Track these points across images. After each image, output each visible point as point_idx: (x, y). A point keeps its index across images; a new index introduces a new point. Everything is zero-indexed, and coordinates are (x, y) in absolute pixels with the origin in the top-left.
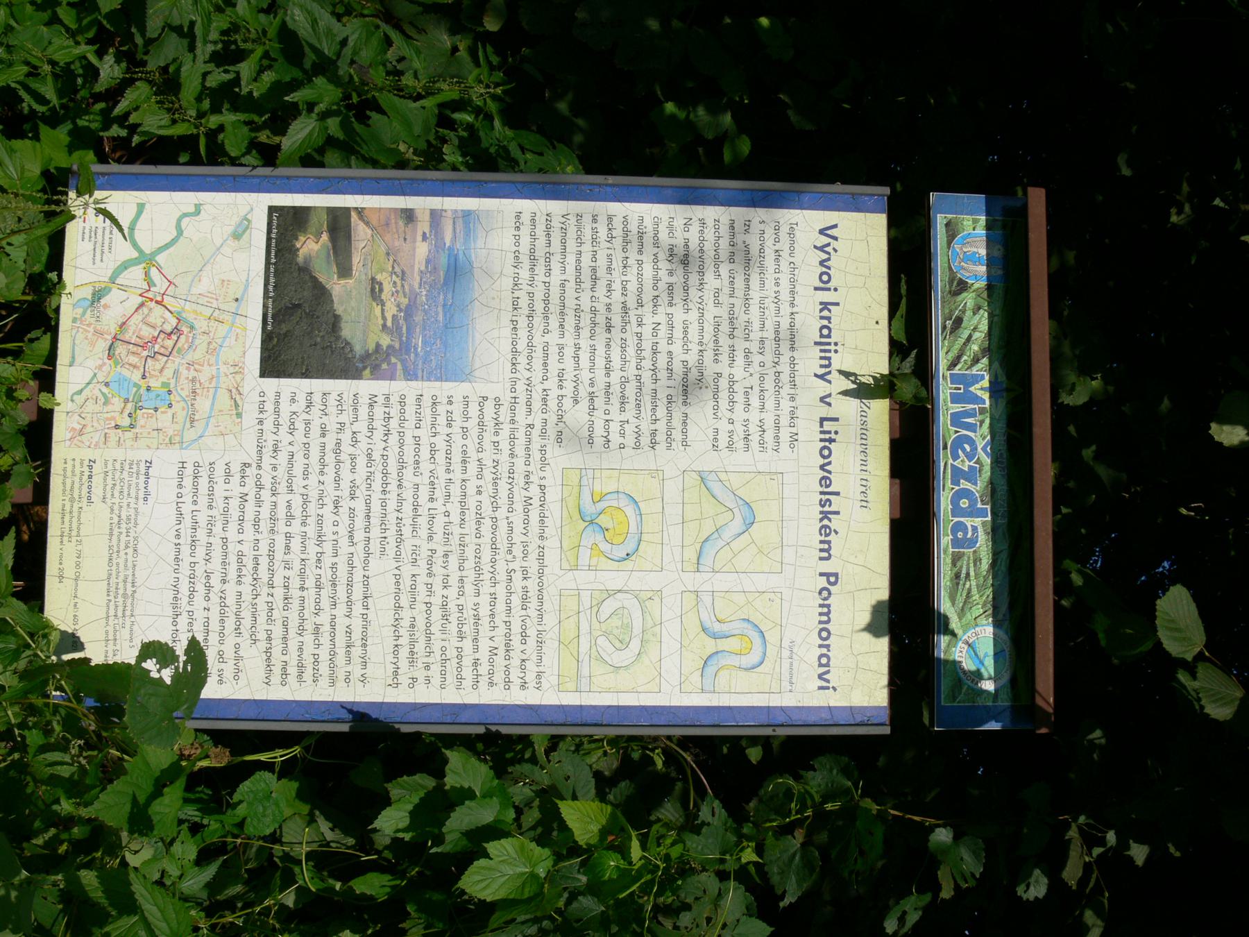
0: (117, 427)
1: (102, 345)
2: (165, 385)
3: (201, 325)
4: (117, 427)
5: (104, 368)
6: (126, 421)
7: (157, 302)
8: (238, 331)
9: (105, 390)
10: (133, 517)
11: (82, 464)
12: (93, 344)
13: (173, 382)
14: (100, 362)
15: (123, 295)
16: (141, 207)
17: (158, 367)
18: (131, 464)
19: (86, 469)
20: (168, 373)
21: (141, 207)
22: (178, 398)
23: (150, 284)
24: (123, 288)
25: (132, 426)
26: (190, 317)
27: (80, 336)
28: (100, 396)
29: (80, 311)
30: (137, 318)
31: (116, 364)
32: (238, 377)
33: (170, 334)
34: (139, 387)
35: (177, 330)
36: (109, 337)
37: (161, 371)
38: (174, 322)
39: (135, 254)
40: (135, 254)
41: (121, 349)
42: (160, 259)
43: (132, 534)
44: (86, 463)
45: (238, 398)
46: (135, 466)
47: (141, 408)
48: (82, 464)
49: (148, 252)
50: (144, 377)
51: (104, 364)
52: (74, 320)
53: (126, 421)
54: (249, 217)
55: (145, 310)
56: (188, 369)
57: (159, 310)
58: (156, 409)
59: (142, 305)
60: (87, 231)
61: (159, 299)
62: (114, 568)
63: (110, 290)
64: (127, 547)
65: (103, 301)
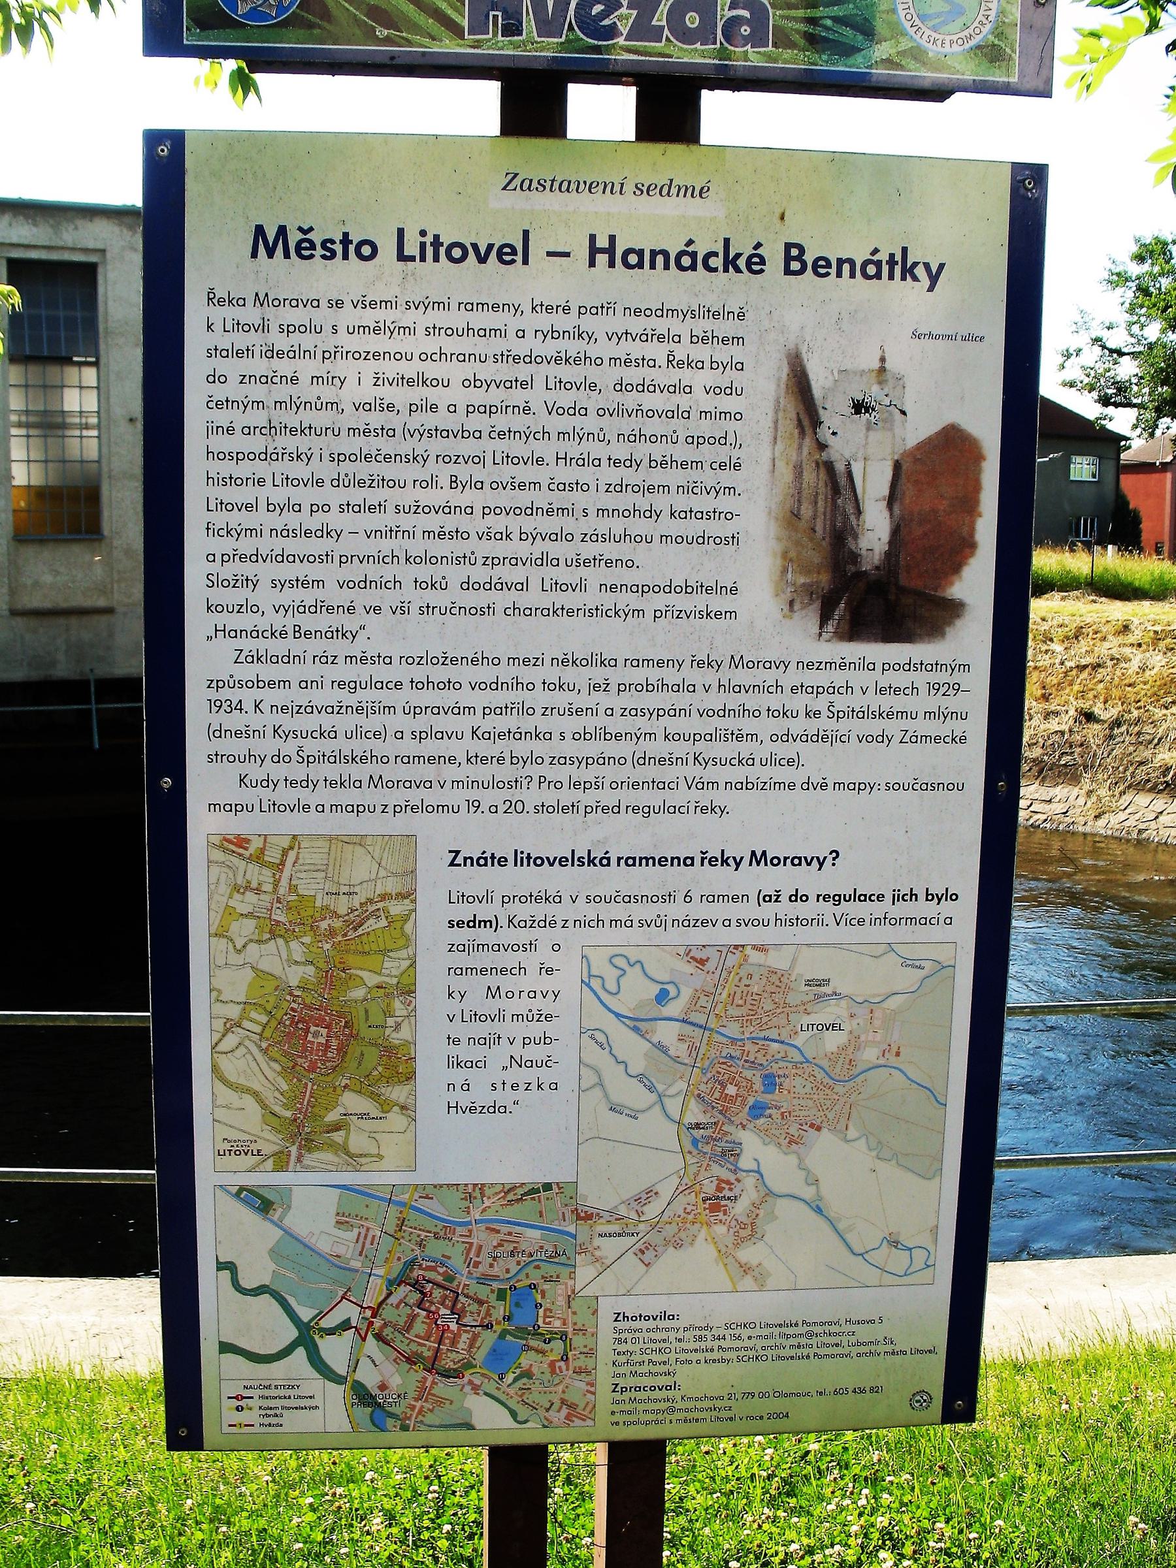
0: (565, 1358)
1: (443, 1388)
2: (501, 1295)
3: (408, 1250)
4: (565, 1358)
5: (477, 1382)
6: (558, 1345)
7: (374, 1316)
8: (416, 1196)
9: (510, 1377)
10: (698, 1333)
11: (618, 1402)
12: (440, 1402)
13: (496, 1285)
14: (468, 1388)
15: (364, 1363)
16: (226, 1348)
17: (475, 1307)
18: (619, 1340)
19: (626, 1396)
20: (483, 1292)
21: (226, 1348)
22: (522, 1276)
23: (345, 1325)
24: (354, 1366)
25: (563, 1336)
26: (397, 1268)
27: (429, 1418)
28: (519, 1384)
29: (390, 1422)
30: (400, 1343)
31: (469, 1365)
32: (488, 1192)
33: (424, 1294)
34: (504, 1333)
35: (416, 1285)
36: (430, 1379)
37: (481, 1303)
38: (403, 1290)
39: (300, 1352)
40: (300, 1352)
41: (448, 1361)
42: (305, 1314)
43: (722, 1332)
44: (617, 1396)
45: (520, 1191)
46: (623, 1336)
47: (536, 1326)
48: (618, 1402)
49: (294, 1333)
50: (489, 1326)
51: (470, 1382)
52: (405, 1428)
53: (558, 1345)
54: (234, 1190)
55: (387, 1331)
56: (477, 1265)
57: (388, 1313)
58: (538, 1306)
59: (379, 1337)
60: (267, 1421)
61: (369, 1313)
62: (769, 1352)
63: (355, 1381)
64: (739, 1338)
65: (375, 1391)
